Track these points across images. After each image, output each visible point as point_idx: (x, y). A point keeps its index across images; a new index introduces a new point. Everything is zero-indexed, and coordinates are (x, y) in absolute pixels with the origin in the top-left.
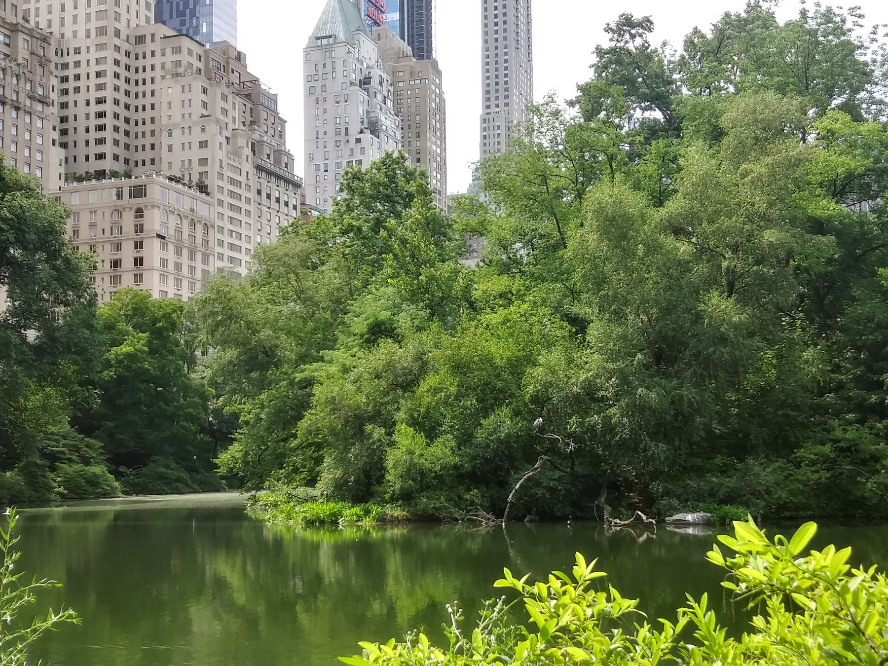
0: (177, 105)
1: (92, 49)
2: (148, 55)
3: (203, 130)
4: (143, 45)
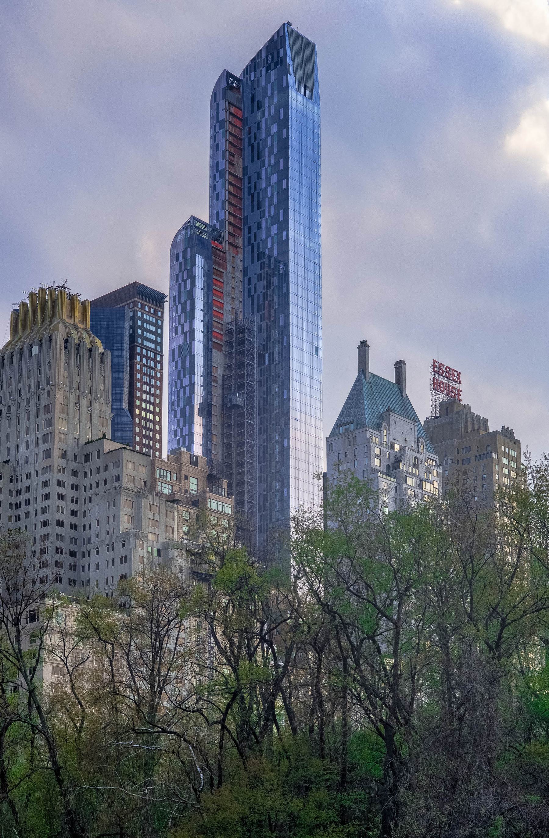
0: (103, 521)
1: (40, 472)
2: (95, 471)
3: (124, 545)
4: (90, 463)
